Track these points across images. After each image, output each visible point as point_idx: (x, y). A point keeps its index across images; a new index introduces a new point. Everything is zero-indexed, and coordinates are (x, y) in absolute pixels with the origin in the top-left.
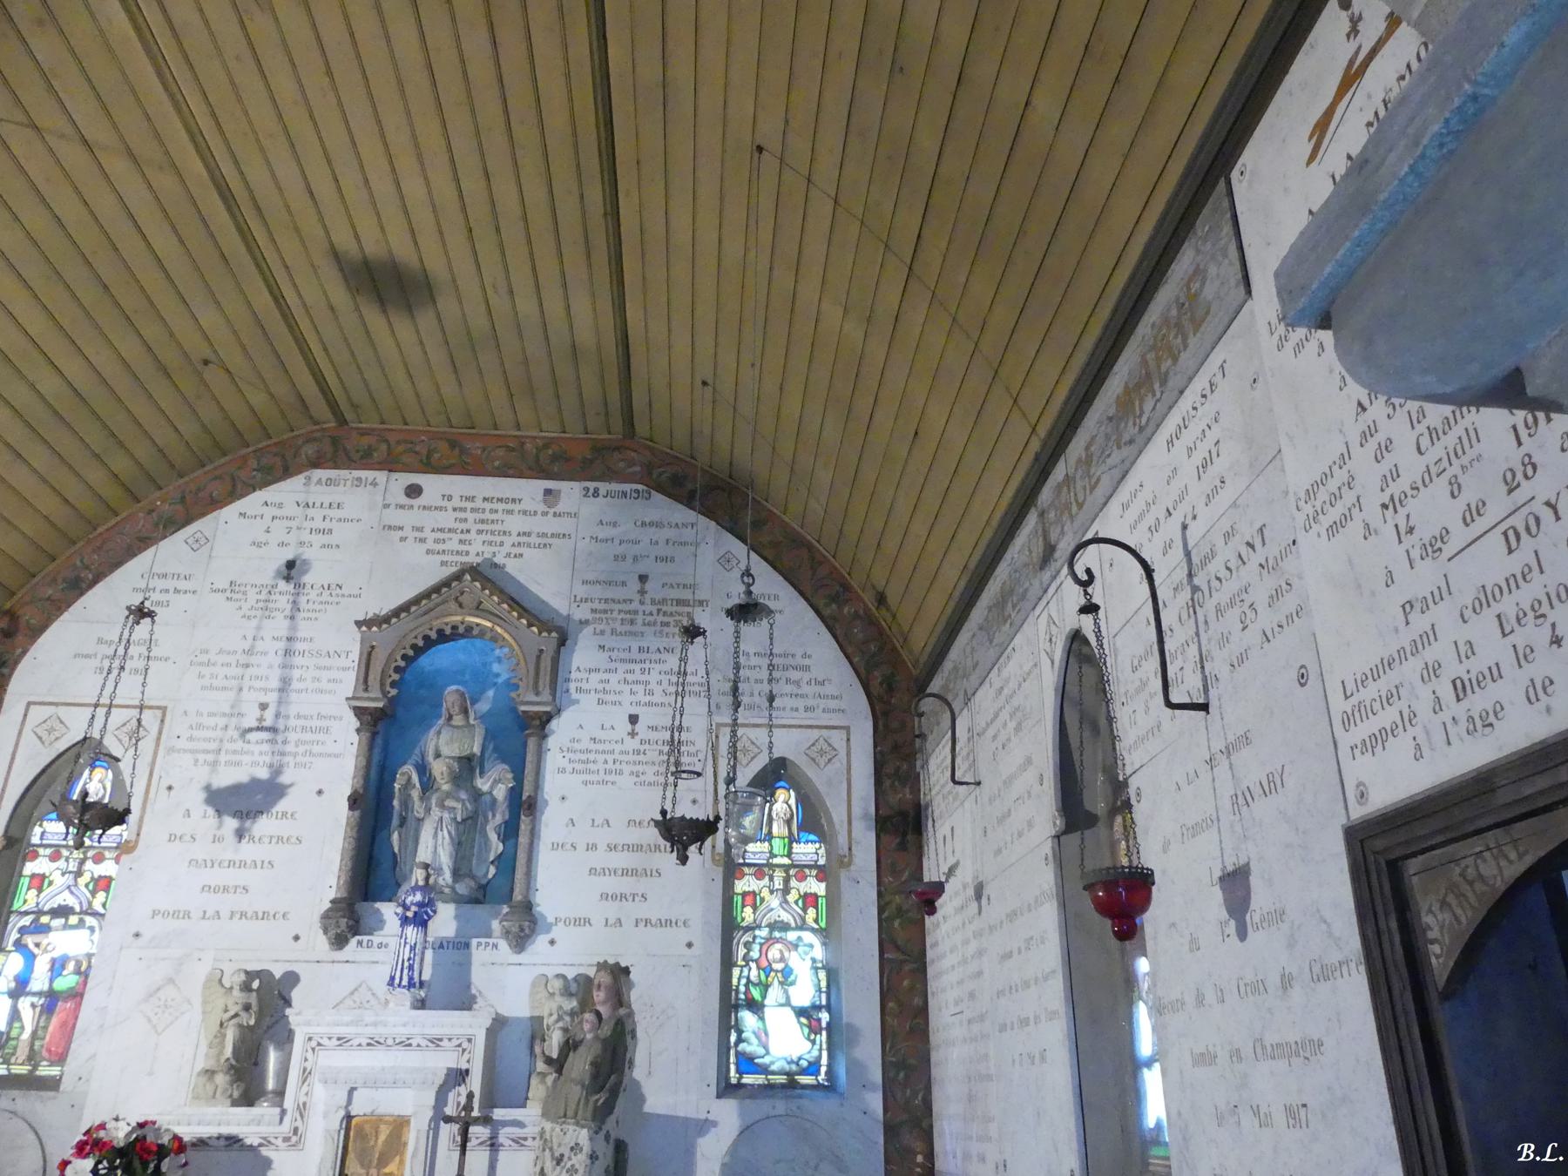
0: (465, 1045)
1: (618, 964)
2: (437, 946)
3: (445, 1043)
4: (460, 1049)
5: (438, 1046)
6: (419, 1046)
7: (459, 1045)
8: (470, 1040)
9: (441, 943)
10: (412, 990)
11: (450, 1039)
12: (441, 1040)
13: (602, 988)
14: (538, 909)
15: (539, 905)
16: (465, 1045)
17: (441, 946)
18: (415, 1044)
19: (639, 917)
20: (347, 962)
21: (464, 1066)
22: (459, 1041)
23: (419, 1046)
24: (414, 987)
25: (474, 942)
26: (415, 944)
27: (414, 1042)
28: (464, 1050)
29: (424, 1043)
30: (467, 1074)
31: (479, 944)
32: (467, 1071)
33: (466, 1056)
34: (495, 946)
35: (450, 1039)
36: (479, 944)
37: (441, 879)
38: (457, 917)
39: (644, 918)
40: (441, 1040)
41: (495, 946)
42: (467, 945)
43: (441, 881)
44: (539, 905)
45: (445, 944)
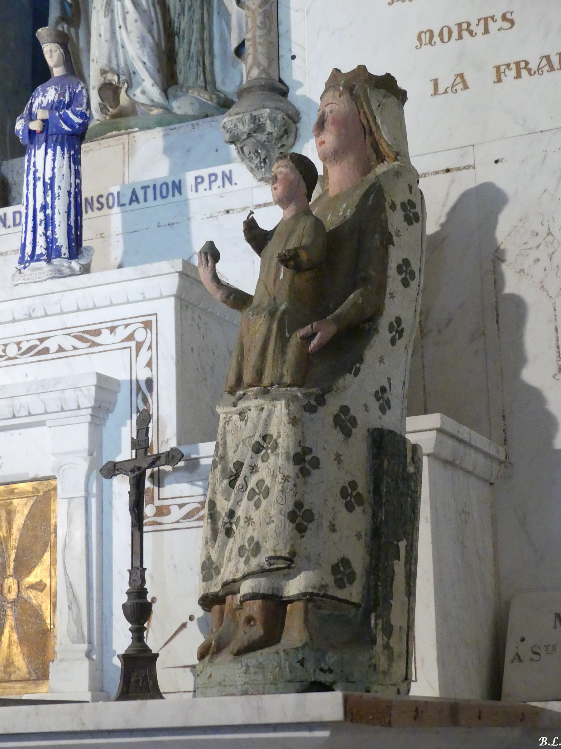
0: (140, 335)
1: (362, 69)
2: (126, 200)
3: (105, 337)
4: (133, 344)
5: (94, 344)
6: (61, 349)
7: (131, 337)
8: (147, 325)
9: (134, 192)
10: (56, 261)
11: (112, 329)
12: (97, 333)
13: (329, 126)
14: (299, 92)
15: (300, 85)
16: (140, 335)
17: (134, 198)
18: (54, 348)
19: (502, 60)
20: (114, 343)
21: (143, 374)
22: (130, 330)
23: (61, 349)
24: (59, 256)
25: (189, 178)
26: (52, 179)
27: (52, 344)
28: (139, 346)
29: (69, 342)
30: (150, 389)
31: (199, 180)
32: (149, 382)
33: (145, 355)
34: (228, 178)
35: (112, 329)
36: (199, 180)
37: (138, 92)
38: (168, 150)
39: (512, 60)
40: (97, 333)
41: (228, 178)
42: (178, 187)
43: (140, 98)
44: (300, 85)
45: (140, 194)
